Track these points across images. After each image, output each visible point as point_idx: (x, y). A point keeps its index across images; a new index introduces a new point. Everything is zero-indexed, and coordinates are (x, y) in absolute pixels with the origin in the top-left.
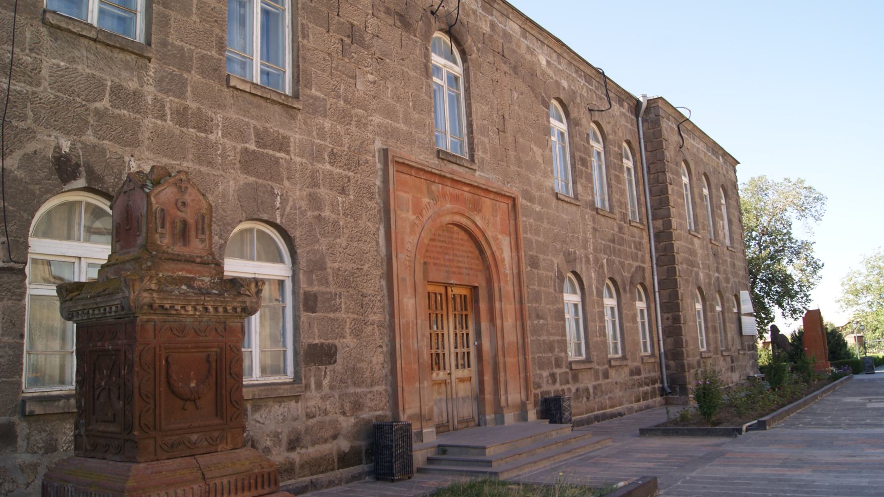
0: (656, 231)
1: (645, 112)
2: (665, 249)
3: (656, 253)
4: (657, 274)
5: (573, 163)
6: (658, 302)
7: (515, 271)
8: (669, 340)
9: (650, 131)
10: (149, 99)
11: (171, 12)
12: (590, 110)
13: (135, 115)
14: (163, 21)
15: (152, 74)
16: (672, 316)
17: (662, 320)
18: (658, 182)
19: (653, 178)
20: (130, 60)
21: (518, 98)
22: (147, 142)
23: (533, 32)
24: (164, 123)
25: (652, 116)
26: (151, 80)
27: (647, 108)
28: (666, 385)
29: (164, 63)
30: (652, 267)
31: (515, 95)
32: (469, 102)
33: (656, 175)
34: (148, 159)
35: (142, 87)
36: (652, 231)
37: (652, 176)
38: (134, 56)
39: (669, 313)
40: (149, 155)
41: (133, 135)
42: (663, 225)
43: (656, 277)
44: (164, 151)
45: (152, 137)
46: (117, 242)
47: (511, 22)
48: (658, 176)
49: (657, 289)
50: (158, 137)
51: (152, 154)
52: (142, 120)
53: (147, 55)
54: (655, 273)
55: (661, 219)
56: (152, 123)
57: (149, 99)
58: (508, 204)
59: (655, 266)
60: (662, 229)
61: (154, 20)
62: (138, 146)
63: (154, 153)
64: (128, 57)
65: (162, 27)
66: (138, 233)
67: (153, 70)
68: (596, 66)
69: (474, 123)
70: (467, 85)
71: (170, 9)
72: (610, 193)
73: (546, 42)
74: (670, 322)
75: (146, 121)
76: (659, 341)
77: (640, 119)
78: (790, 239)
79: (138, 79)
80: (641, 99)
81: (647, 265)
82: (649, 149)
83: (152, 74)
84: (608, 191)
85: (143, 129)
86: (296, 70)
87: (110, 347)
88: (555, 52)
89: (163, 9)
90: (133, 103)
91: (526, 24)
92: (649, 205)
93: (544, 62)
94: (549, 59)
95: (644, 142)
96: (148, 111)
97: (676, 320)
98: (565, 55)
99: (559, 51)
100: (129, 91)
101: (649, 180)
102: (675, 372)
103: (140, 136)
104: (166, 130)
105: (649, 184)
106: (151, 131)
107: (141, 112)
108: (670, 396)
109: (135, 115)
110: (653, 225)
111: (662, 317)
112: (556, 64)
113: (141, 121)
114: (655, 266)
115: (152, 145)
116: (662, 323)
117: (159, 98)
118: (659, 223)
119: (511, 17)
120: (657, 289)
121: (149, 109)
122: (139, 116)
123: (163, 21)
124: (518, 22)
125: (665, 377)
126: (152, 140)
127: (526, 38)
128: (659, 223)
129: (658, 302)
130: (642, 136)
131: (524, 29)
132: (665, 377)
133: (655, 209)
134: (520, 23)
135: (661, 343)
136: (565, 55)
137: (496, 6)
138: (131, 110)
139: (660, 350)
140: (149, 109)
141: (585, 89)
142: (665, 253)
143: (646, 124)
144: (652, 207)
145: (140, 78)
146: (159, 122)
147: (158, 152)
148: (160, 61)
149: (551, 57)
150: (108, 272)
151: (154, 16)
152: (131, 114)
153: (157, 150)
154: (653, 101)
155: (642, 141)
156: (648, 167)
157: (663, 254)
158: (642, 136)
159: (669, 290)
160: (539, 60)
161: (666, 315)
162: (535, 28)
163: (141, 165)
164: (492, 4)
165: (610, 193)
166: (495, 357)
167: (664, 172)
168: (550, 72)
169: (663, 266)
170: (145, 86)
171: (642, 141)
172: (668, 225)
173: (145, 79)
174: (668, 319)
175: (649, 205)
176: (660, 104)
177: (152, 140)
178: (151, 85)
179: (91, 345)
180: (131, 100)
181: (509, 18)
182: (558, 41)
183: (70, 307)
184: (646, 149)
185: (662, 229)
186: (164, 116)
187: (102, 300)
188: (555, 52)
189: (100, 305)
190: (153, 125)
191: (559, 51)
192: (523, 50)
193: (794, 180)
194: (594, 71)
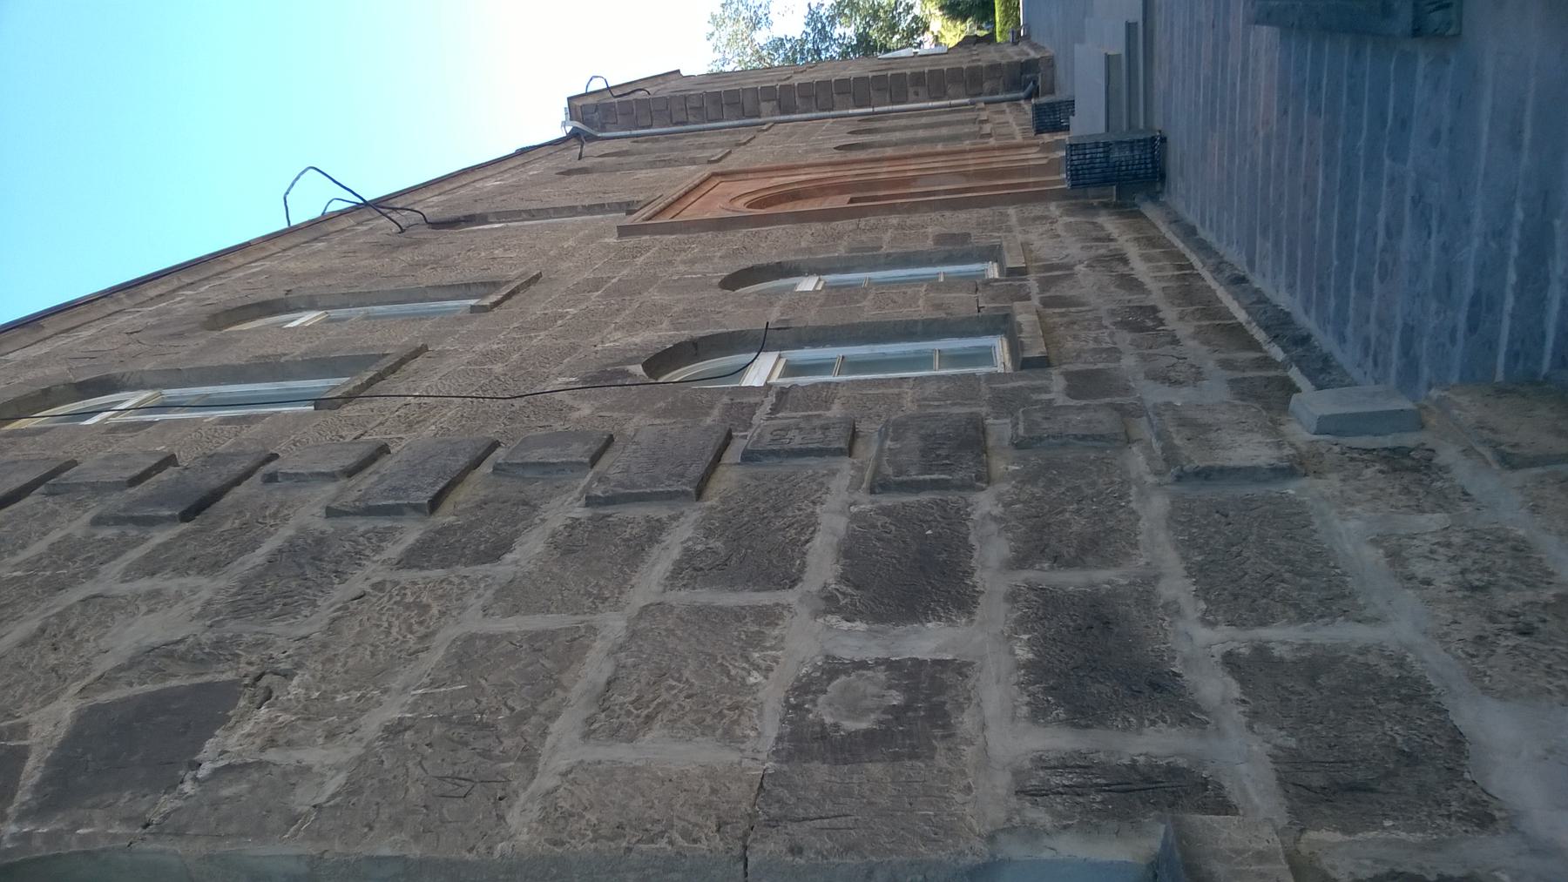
0: (778, 111)
2: (805, 97)
3: (811, 112)
5: (663, 163)
6: (890, 108)
7: (829, 169)
8: (950, 92)
12: (580, 158)
16: (912, 86)
18: (700, 108)
28: (1022, 94)
30: (833, 117)
32: (552, 211)
36: (777, 118)
37: (691, 119)
39: (907, 92)
42: (769, 101)
43: (850, 111)
48: (691, 108)
49: (871, 110)
54: (845, 112)
55: (759, 104)
59: (832, 113)
60: (775, 103)
68: (512, 151)
69: (587, 202)
70: (524, 216)
74: (921, 90)
76: (951, 106)
77: (599, 135)
78: (803, 42)
80: (569, 129)
81: (831, 120)
82: (649, 122)
86: (474, 290)
92: (736, 122)
97: (918, 78)
102: (1001, 81)
108: (1039, 83)
110: (767, 116)
111: (913, 102)
114: (832, 113)
116: (924, 101)
118: (765, 107)
120: (871, 110)
125: (1009, 96)
128: (765, 107)
129: (890, 108)
130: (628, 133)
132: (1009, 96)
135: (953, 102)
139: (966, 105)
142: (814, 98)
143: (608, 127)
144: (738, 119)
154: (573, 112)
156: (677, 124)
158: (628, 133)
161: (911, 96)
162: (442, 184)
166: (965, 175)
167: (685, 98)
174: (917, 94)
175: (736, 122)
176: (579, 103)
184: (649, 127)
185: (775, 103)
193: (711, 28)
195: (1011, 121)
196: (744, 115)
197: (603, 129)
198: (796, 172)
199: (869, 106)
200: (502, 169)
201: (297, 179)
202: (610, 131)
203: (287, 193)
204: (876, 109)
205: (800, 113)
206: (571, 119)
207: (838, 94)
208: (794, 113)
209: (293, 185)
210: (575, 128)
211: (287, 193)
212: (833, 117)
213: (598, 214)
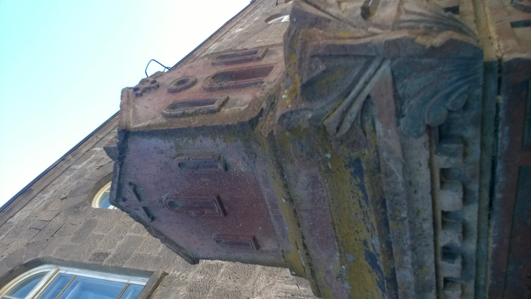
10: (199, 277)
11: (134, 253)
12: (277, 4)
13: (211, 292)
14: (138, 260)
15: (179, 273)
20: (161, 291)
21: (260, 39)
22: (238, 284)
23: (220, 36)
24: (224, 266)
26: (184, 274)
29: (173, 262)
31: (258, 41)
34: (254, 284)
35: (187, 283)
38: (159, 288)
40: (251, 282)
41: (229, 296)
44: (250, 269)
45: (234, 278)
46: (258, 247)
47: (210, 47)
50: (236, 273)
51: (251, 280)
52: (216, 286)
53: (160, 276)
56: (222, 277)
57: (199, 277)
61: (136, 268)
62: (240, 292)
63: (250, 278)
64: (158, 293)
65: (143, 261)
66: (220, 167)
67: (176, 272)
68: (249, 3)
71: (132, 253)
73: (227, 30)
75: (219, 282)
79: (179, 286)
83: (179, 273)
85: (225, 286)
88: (235, 25)
89: (129, 259)
90: (199, 292)
91: (213, 39)
93: (240, 30)
94: (239, 27)
96: (210, 280)
98: (238, 20)
99: (235, 23)
100: (187, 296)
103: (230, 290)
104: (231, 265)
106: (228, 278)
107: (210, 287)
109: (211, 292)
112: (243, 24)
113: (217, 287)
115: (242, 279)
117: (200, 269)
119: (206, 47)
121: (209, 278)
122: (212, 289)
123: (138, 260)
124: (211, 44)
126: (237, 278)
127: (222, 40)
131: (216, 41)
134: (212, 43)
136: (238, 20)
137: (197, 55)
138: (205, 296)
140: (209, 278)
141: (263, 9)
145: (180, 284)
146: (222, 270)
147: (249, 274)
148: (170, 265)
149: (238, 27)
150: (328, 272)
151: (132, 267)
152: (208, 295)
153: (247, 275)
160: (238, 32)
162: (216, 35)
163: (259, 291)
164: (196, 57)
168: (247, 26)
170: (187, 280)
173: (181, 279)
177: (237, 278)
178: (188, 275)
180: (196, 294)
181: (208, 48)
182: (227, 23)
186: (217, 266)
187: (408, 259)
188: (235, 25)
189: (430, 277)
190: (224, 277)
191: (235, 23)
192: (230, 40)
194: (252, 5)
200: (244, 15)
201: (148, 64)
203: (146, 70)
209: (147, 67)
211: (146, 70)
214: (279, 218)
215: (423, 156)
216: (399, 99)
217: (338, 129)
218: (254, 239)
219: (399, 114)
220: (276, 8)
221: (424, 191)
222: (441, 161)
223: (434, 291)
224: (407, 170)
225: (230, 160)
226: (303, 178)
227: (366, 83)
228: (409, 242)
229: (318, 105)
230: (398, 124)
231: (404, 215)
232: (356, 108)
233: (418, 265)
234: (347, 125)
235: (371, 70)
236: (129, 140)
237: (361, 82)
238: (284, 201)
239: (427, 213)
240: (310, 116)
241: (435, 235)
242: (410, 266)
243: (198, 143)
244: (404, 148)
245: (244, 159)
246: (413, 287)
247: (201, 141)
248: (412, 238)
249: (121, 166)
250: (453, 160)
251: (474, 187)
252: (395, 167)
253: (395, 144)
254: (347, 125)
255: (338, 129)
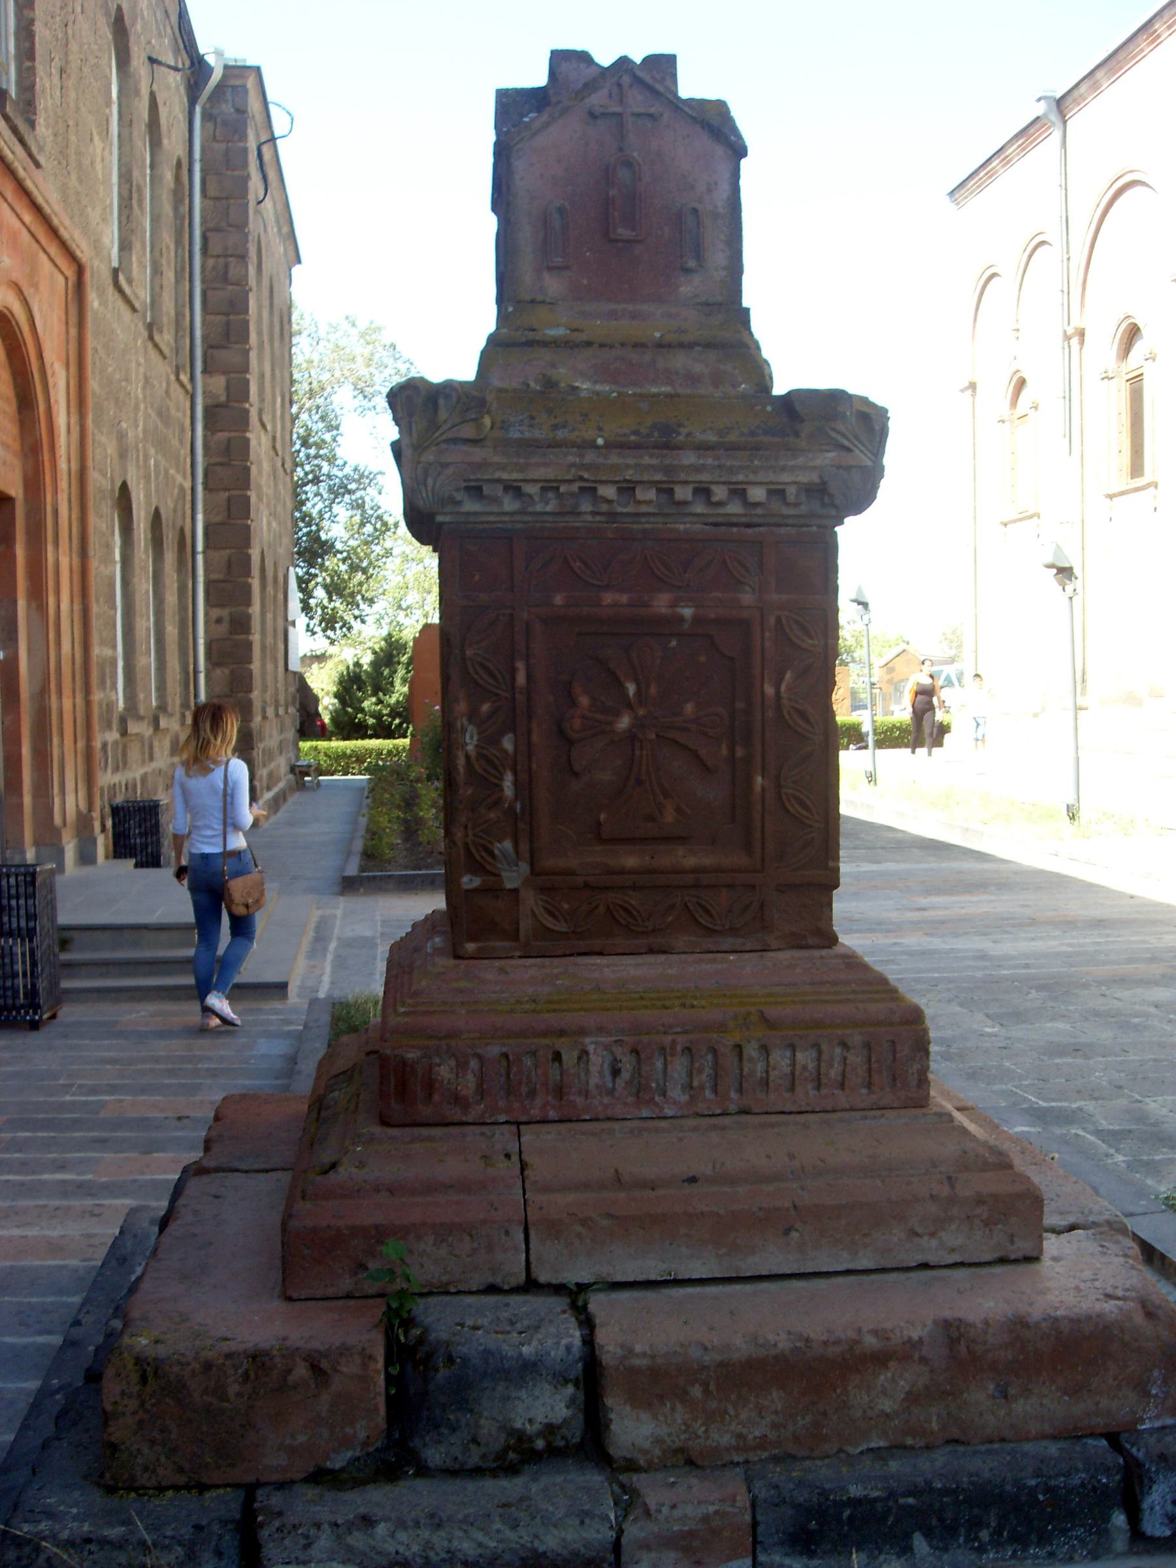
0: (210, 402)
1: (210, 99)
4: (205, 506)
5: (126, 194)
6: (201, 579)
7: (75, 466)
8: (218, 672)
9: (216, 145)
12: (152, 61)
16: (231, 614)
17: (206, 622)
18: (225, 278)
19: (214, 268)
25: (227, 108)
27: (220, 87)
30: (193, 489)
33: (221, 260)
36: (199, 401)
37: (211, 262)
42: (228, 388)
43: (200, 517)
46: (550, 269)
48: (227, 265)
49: (200, 547)
55: (224, 373)
58: (66, 279)
60: (223, 398)
66: (692, 264)
72: (157, 289)
74: (223, 629)
76: (196, 672)
77: (198, 109)
78: (331, 460)
80: (211, 60)
81: (187, 485)
82: (212, 192)
84: (152, 281)
87: (687, 612)
92: (198, 333)
95: (202, 170)
97: (241, 624)
101: (203, 267)
105: (203, 281)
110: (205, 385)
111: (206, 614)
114: (200, 488)
116: (206, 632)
118: (219, 382)
120: (200, 547)
128: (219, 382)
129: (201, 579)
130: (197, 155)
133: (211, 347)
135: (202, 677)
142: (225, 460)
143: (210, 125)
144: (205, 338)
150: (553, 365)
155: (197, 167)
156: (205, 239)
157: (219, 460)
158: (197, 155)
159: (228, 551)
161: (216, 613)
165: (157, 289)
166: (42, 693)
169: (217, 490)
171: (197, 167)
172: (239, 391)
174: (219, 621)
175: (198, 333)
176: (251, 83)
179: (558, 600)
183: (483, 465)
185: (223, 398)
187: (709, 461)
193: (362, 325)
195: (154, 765)
196: (210, 346)
197: (207, 117)
198: (73, 410)
199: (207, 546)
202: (203, 126)
204: (200, 559)
205: (205, 437)
206: (226, 67)
207: (229, 499)
208: (206, 428)
210: (209, 70)
212: (193, 489)
213: (17, 47)
214: (613, 315)
215: (804, 478)
216: (848, 468)
217: (834, 430)
218: (566, 268)
219: (839, 467)
220: (144, 57)
221: (772, 477)
222: (791, 491)
223: (664, 479)
224: (793, 468)
225: (697, 279)
226: (698, 368)
227: (862, 451)
228: (729, 463)
229: (854, 420)
230: (832, 466)
231: (756, 462)
232: (846, 443)
233: (699, 469)
234: (834, 435)
235: (869, 455)
236: (730, 152)
237: (862, 448)
238: (657, 335)
239: (752, 478)
240: (848, 414)
241: (724, 483)
242: (701, 462)
243: (721, 246)
244: (814, 468)
245: (696, 296)
246: (676, 462)
247: (723, 251)
248: (732, 467)
249: (694, 119)
250: (792, 497)
251: (759, 511)
252: (800, 461)
253: (818, 462)
254: (834, 435)
255: (834, 430)
